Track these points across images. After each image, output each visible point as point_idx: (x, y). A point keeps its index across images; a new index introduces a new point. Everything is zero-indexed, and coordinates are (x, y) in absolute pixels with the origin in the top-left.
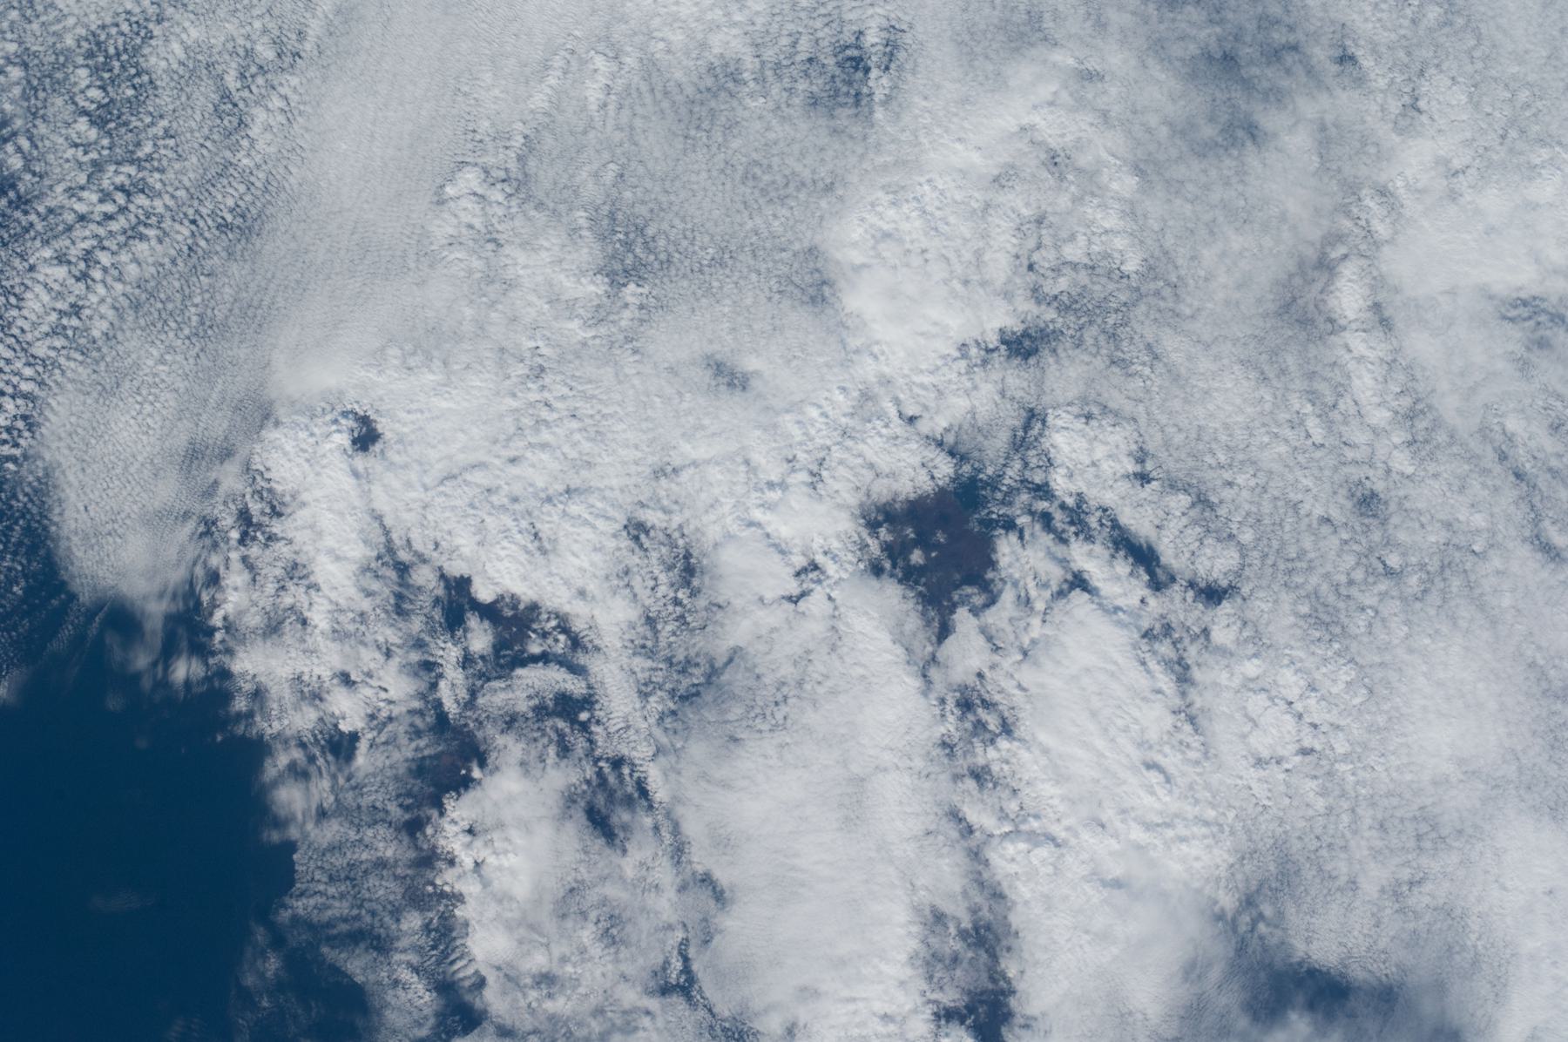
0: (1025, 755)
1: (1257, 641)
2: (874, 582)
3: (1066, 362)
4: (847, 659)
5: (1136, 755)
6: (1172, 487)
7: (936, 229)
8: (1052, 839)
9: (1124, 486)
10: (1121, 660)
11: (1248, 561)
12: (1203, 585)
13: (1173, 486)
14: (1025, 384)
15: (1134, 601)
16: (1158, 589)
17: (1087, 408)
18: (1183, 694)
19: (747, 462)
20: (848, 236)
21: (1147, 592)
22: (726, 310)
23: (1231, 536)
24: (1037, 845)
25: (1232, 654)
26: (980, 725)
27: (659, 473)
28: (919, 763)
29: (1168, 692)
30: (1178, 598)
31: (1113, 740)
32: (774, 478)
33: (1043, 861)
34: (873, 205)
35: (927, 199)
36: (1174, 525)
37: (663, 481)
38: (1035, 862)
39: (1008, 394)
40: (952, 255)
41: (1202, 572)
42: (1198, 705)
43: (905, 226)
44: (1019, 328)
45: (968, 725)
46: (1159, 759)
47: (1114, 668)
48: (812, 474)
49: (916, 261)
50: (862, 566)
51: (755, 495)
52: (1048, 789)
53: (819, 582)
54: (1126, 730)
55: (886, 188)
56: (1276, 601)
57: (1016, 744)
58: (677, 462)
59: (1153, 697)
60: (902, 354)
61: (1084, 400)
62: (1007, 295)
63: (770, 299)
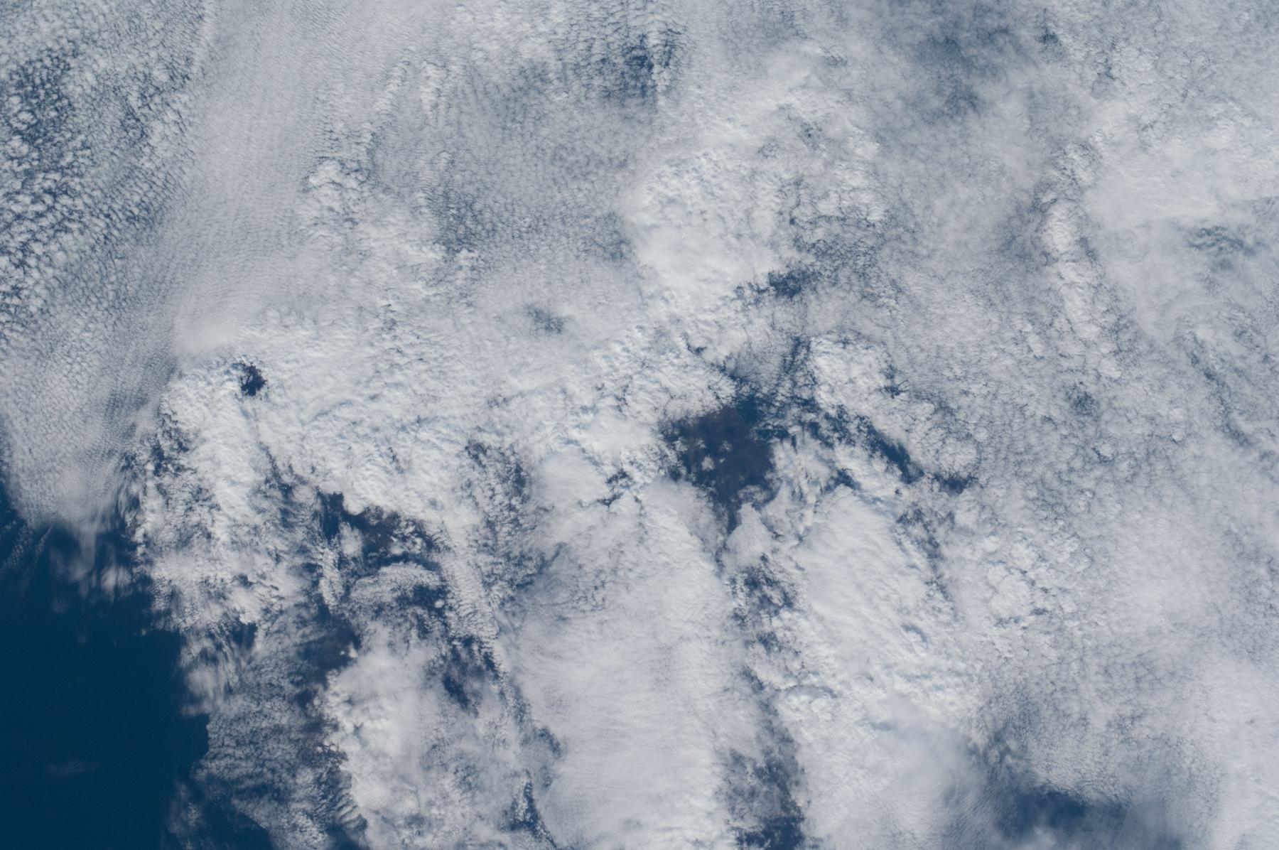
0: (804, 623)
1: (994, 521)
2: (673, 486)
4: (653, 550)
5: (896, 619)
6: (917, 397)
7: (712, 194)
8: (831, 692)
9: (877, 399)
11: (983, 455)
12: (946, 477)
13: (918, 396)
14: (791, 318)
15: (890, 492)
18: (934, 568)
19: (564, 391)
20: (639, 204)
21: (900, 485)
22: (542, 267)
23: (969, 436)
24: (816, 696)
25: (973, 534)
26: (765, 600)
27: (493, 403)
28: (715, 633)
30: (926, 488)
31: (876, 608)
32: (587, 403)
33: (822, 710)
35: (704, 169)
36: (920, 429)
37: (496, 410)
38: (816, 711)
39: (778, 326)
40: (726, 215)
41: (945, 466)
42: (947, 576)
43: (687, 192)
45: (756, 600)
46: (916, 622)
47: (875, 548)
48: (618, 399)
49: (697, 221)
50: (662, 473)
51: (571, 418)
52: (824, 650)
53: (628, 487)
54: (887, 599)
55: (670, 162)
56: (1008, 488)
57: (796, 614)
58: (507, 393)
60: (688, 298)
61: (841, 329)
62: (773, 245)
63: (577, 257)
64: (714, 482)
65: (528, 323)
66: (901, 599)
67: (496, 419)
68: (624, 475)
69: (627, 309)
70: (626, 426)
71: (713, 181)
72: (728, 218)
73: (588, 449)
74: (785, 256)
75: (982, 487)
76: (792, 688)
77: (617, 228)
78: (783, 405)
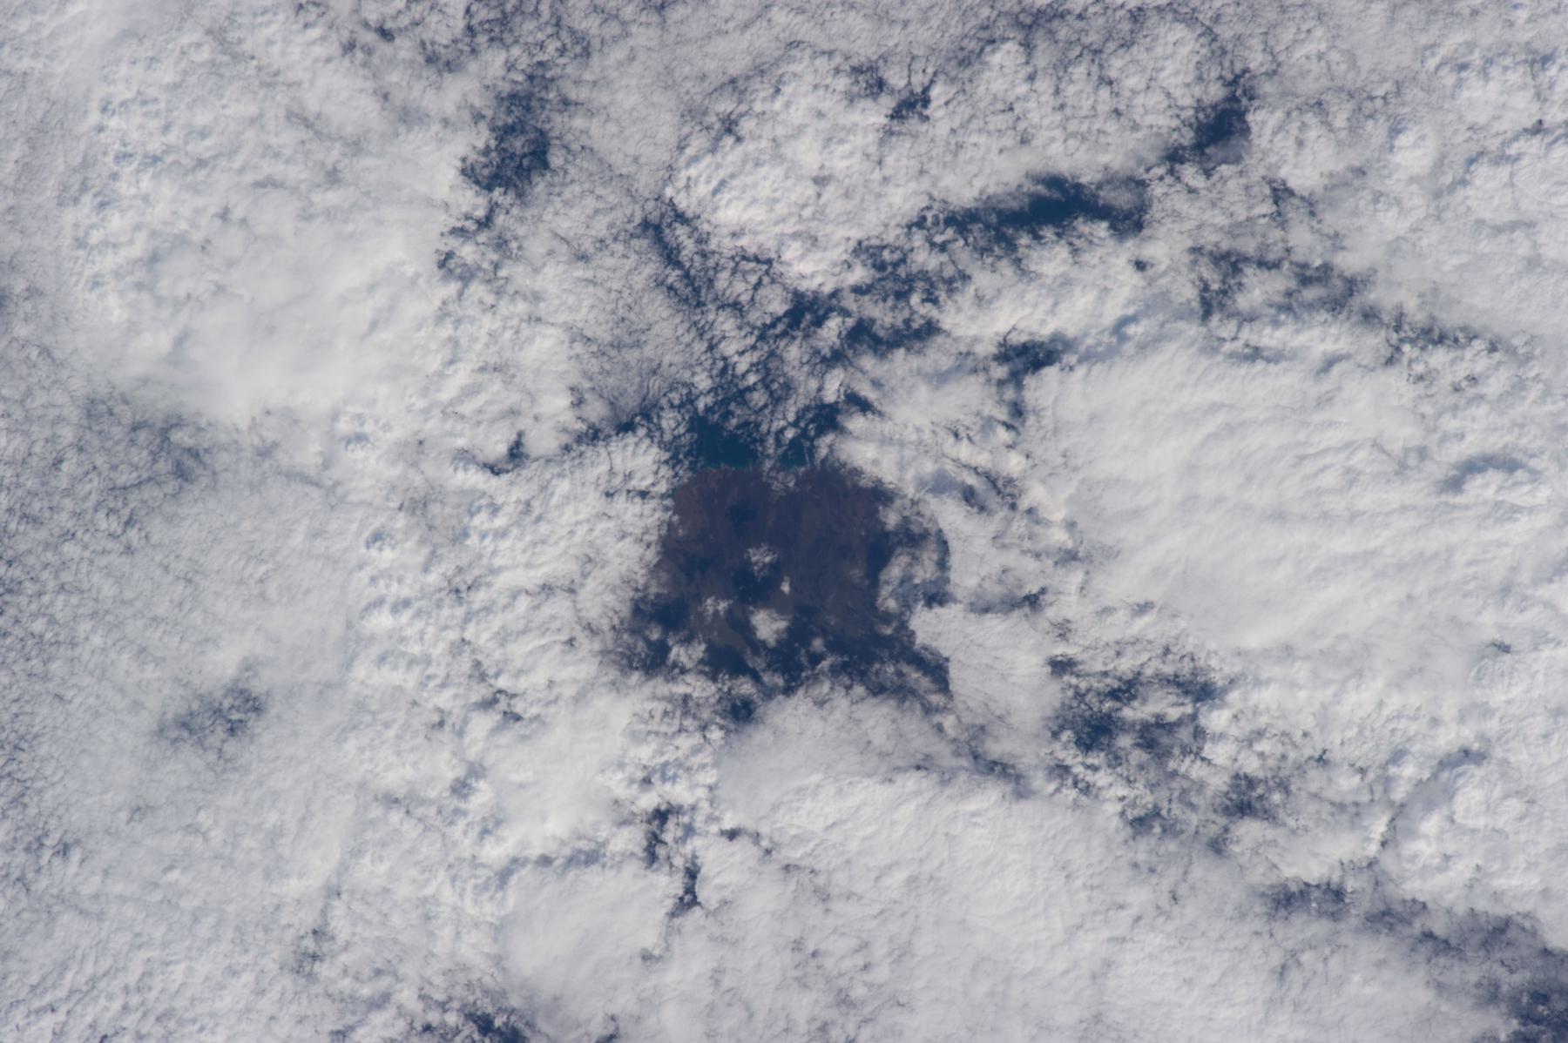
0: (1266, 697)
2: (759, 736)
3: (603, 98)
4: (859, 888)
5: (1414, 492)
7: (201, 163)
8: (1466, 755)
9: (900, 156)
10: (1215, 395)
12: (1188, 138)
16: (1139, 226)
17: (712, 119)
18: (1370, 316)
19: (391, 801)
20: (112, 329)
22: (97, 640)
24: (1449, 794)
25: (1361, 172)
26: (1153, 737)
28: (1140, 897)
29: (1342, 346)
30: (1179, 201)
31: (1354, 516)
35: (135, 135)
36: (1039, 112)
39: (587, 246)
40: (268, 168)
41: (1165, 122)
42: (1411, 305)
43: (159, 213)
44: (482, 137)
45: (1138, 756)
46: (1456, 452)
47: (1221, 418)
48: (488, 704)
49: (231, 242)
50: (716, 735)
51: (457, 831)
52: (1359, 700)
53: (689, 830)
54: (1352, 477)
57: (1234, 696)
58: (309, 918)
59: (1327, 385)
60: (384, 390)
61: (693, 114)
62: (408, 117)
63: (129, 550)
64: (818, 644)
65: (186, 764)
66: (1376, 445)
68: (661, 816)
69: (316, 534)
70: (559, 734)
71: (172, 137)
72: (277, 169)
73: (550, 848)
74: (449, 108)
77: (127, 419)
78: (762, 367)
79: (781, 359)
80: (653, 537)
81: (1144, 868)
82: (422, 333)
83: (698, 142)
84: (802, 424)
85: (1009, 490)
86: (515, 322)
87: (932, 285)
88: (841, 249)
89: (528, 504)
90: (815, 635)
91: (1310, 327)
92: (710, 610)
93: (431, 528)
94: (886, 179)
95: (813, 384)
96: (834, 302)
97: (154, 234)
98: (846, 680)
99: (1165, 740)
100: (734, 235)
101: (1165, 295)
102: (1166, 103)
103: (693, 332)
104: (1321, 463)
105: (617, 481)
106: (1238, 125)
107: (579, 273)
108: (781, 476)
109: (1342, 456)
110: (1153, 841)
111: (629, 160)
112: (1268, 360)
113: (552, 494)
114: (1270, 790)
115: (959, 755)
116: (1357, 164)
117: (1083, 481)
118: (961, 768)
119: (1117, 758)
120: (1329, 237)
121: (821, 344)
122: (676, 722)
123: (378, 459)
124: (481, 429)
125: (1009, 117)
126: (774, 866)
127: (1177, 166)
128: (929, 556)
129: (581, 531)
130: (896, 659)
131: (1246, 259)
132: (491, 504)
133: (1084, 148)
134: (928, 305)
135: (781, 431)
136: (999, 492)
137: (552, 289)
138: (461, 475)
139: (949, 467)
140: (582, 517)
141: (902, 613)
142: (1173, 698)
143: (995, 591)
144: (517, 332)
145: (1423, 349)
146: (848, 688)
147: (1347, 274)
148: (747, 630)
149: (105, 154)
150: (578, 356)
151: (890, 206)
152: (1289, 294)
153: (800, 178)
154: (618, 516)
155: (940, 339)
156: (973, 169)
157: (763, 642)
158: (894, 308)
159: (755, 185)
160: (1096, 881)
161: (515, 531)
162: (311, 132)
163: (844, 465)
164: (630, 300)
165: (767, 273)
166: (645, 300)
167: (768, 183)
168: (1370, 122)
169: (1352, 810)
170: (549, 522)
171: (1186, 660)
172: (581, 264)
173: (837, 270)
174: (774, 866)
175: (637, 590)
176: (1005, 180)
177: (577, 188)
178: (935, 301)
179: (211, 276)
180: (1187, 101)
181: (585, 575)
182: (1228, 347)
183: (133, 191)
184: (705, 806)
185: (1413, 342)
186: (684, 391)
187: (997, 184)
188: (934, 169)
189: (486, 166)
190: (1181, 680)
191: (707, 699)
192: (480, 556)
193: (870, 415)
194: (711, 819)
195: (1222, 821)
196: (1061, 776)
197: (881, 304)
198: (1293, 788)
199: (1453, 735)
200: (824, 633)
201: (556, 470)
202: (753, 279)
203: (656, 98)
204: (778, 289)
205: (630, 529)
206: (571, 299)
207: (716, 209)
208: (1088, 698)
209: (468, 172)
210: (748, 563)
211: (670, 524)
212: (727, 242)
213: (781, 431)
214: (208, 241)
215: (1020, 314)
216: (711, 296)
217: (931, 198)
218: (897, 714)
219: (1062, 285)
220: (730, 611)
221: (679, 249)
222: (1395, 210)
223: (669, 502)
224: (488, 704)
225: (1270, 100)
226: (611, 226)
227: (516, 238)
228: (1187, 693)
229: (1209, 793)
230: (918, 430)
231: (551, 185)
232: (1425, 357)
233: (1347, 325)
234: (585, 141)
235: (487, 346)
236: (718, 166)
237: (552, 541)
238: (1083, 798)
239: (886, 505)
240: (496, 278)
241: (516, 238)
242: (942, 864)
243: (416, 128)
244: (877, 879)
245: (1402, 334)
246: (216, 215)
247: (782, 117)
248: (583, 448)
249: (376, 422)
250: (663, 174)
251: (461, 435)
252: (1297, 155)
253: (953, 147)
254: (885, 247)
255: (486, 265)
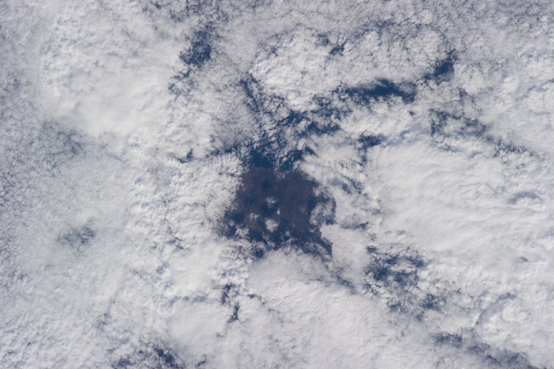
0: (441, 268)
1: (498, 67)
2: (264, 263)
4: (294, 319)
5: (499, 202)
6: (357, 37)
7: (90, 45)
8: (509, 295)
9: (332, 67)
10: (433, 161)
12: (432, 71)
13: (358, 36)
16: (413, 100)
17: (268, 47)
18: (490, 139)
19: (136, 272)
20: (54, 98)
21: (409, 107)
22: (39, 206)
24: (501, 308)
25: (491, 89)
26: (401, 278)
27: (101, 325)
28: (391, 333)
29: (479, 149)
30: (427, 93)
31: (477, 208)
33: (515, 315)
34: (46, 68)
36: (381, 56)
37: (107, 328)
38: (511, 319)
39: (221, 87)
40: (113, 49)
41: (425, 65)
42: (504, 137)
43: (74, 60)
44: (188, 45)
45: (395, 284)
46: (515, 190)
48: (172, 242)
49: (98, 73)
50: (249, 261)
51: (157, 285)
52: (473, 273)
53: (237, 293)
54: (478, 194)
55: (43, 52)
56: (482, 34)
57: (430, 267)
58: (103, 310)
59: (472, 162)
60: (146, 129)
61: (262, 45)
62: (163, 36)
63: (53, 176)
64: (288, 233)
65: (66, 252)
66: (488, 184)
67: (114, 334)
68: (228, 287)
69: (118, 177)
70: (196, 255)
71: (81, 35)
72: (116, 49)
73: (189, 294)
75: (463, 52)
76: (481, 317)
77: (57, 130)
78: (277, 135)
79: (284, 133)
80: (234, 190)
81: (393, 323)
82: (161, 111)
83: (262, 55)
84: (289, 157)
85: (359, 186)
86: (194, 110)
87: (339, 112)
88: (309, 97)
89: (192, 174)
90: (287, 230)
91: (468, 141)
92: (252, 217)
93: (158, 179)
94: (326, 75)
95: (295, 143)
96: (304, 115)
97: (72, 68)
98: (296, 247)
99: (405, 279)
100: (272, 88)
101: (419, 124)
102: (426, 58)
103: (255, 120)
104: (468, 189)
105: (224, 169)
106: (450, 68)
107: (217, 96)
108: (280, 173)
109: (475, 187)
110: (397, 314)
111: (238, 59)
112: (453, 151)
113: (201, 172)
114: (439, 300)
115: (333, 277)
116: (490, 86)
117: (385, 186)
118: (333, 282)
119: (387, 284)
120: (478, 110)
121: (298, 129)
122: (236, 255)
123: (142, 153)
124: (178, 147)
125: (371, 57)
126: (265, 309)
127: (428, 81)
128: (329, 207)
129: (210, 186)
130: (314, 241)
131: (449, 115)
132: (179, 173)
133: (396, 71)
134: (337, 120)
135: (282, 158)
136: (355, 187)
137: (207, 101)
138: (170, 162)
139: (339, 176)
140: (210, 181)
141: (318, 226)
142: (409, 265)
143: (351, 221)
144: (194, 114)
145: (507, 153)
146: (297, 250)
147: (483, 124)
148: (264, 226)
149: (58, 38)
150: (214, 125)
151: (327, 84)
152: (462, 129)
153: (296, 71)
154: (223, 182)
155: (340, 132)
156: (357, 74)
157: (269, 231)
158: (325, 119)
159: (281, 72)
160: (376, 326)
161: (187, 183)
162: (129, 38)
163: (302, 172)
164: (234, 107)
165: (282, 103)
166: (239, 108)
167: (285, 72)
168: (496, 72)
169: (467, 310)
170: (199, 181)
171: (415, 252)
172: (218, 93)
173: (306, 104)
174: (265, 309)
175: (227, 208)
176: (368, 79)
177: (219, 67)
178: (339, 119)
179: (90, 84)
180: (433, 58)
181: (209, 201)
182: (439, 145)
183: (66, 52)
184: (243, 285)
185: (504, 150)
186: (250, 141)
187: (365, 80)
188: (343, 73)
189: (188, 56)
190: (412, 259)
191: (248, 248)
192: (174, 191)
193: (313, 156)
194: (245, 290)
195: (422, 309)
196: (367, 288)
197: (320, 118)
198: (447, 300)
199: (505, 288)
200: (290, 229)
201: (203, 163)
202: (277, 104)
203: (249, 38)
204: (285, 109)
205: (226, 187)
206: (214, 105)
207: (266, 79)
208: (379, 262)
209: (182, 57)
210: (266, 203)
211: (240, 186)
212: (269, 91)
213: (282, 158)
214: (90, 72)
215: (368, 126)
216: (262, 109)
217: (341, 82)
218: (313, 261)
219: (384, 117)
220: (258, 218)
221: (252, 91)
222: (502, 103)
223: (241, 179)
224: (172, 242)
225: (462, 61)
226: (230, 81)
227: (196, 82)
228: (414, 263)
229: (418, 299)
230: (329, 162)
231: (210, 65)
232: (507, 155)
233: (481, 142)
234: (223, 50)
235: (183, 118)
236: (269, 64)
237: (199, 188)
238: (374, 297)
239: (316, 188)
240: (188, 95)
241: (196, 82)
242: (323, 315)
243: (166, 40)
244: (301, 317)
245: (500, 147)
246: (93, 63)
247: (293, 49)
248: (213, 157)
249: (142, 140)
250: (250, 65)
251: (171, 148)
252: (470, 81)
253: (350, 66)
254: (324, 98)
255: (185, 90)
